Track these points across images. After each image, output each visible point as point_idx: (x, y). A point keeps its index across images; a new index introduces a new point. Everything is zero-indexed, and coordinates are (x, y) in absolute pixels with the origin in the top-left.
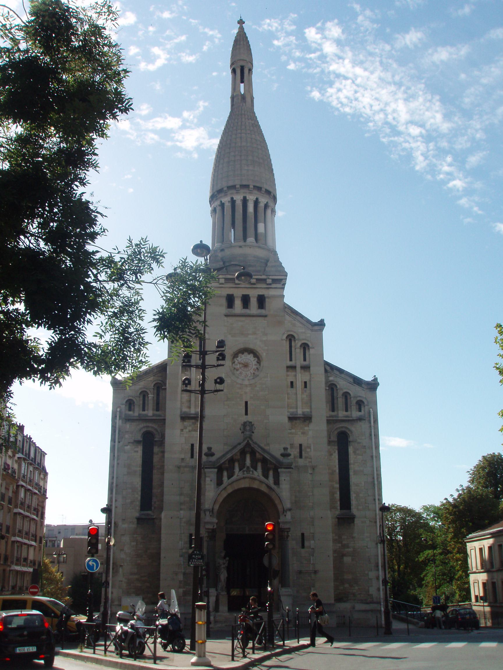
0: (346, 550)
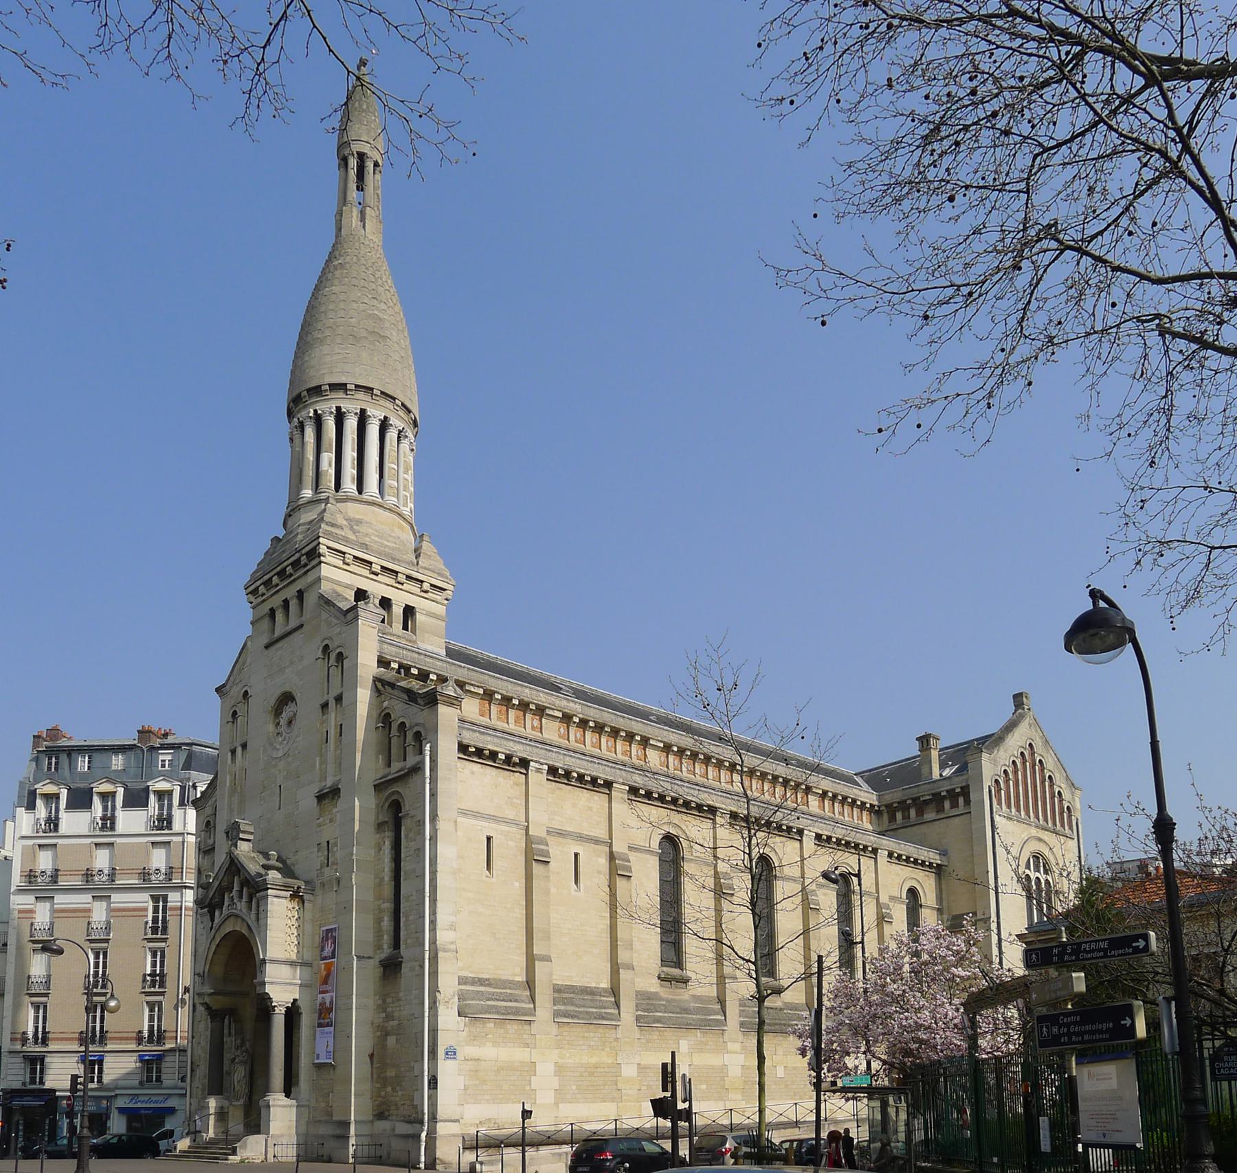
0: (391, 1023)
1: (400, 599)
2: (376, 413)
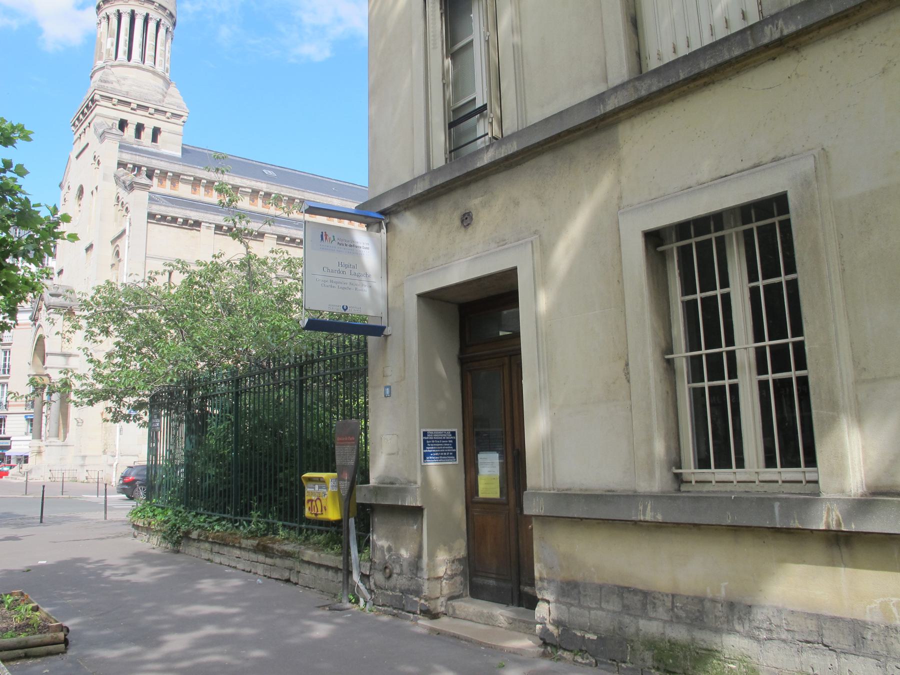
1: (149, 124)
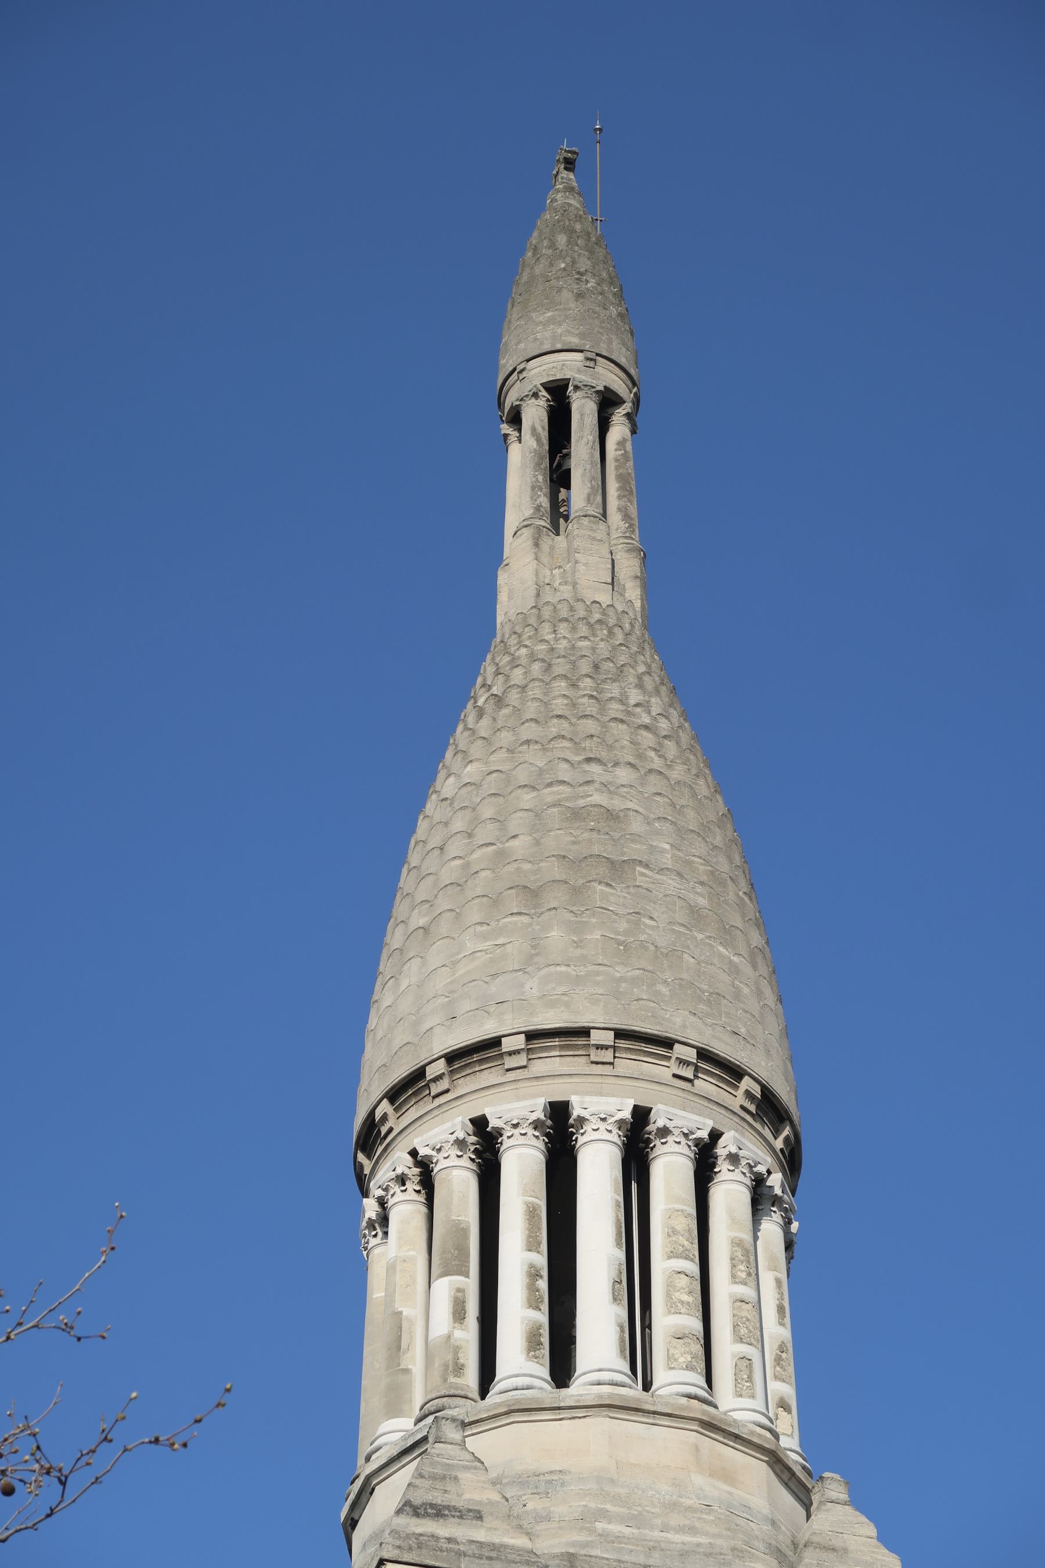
2: (600, 1110)
